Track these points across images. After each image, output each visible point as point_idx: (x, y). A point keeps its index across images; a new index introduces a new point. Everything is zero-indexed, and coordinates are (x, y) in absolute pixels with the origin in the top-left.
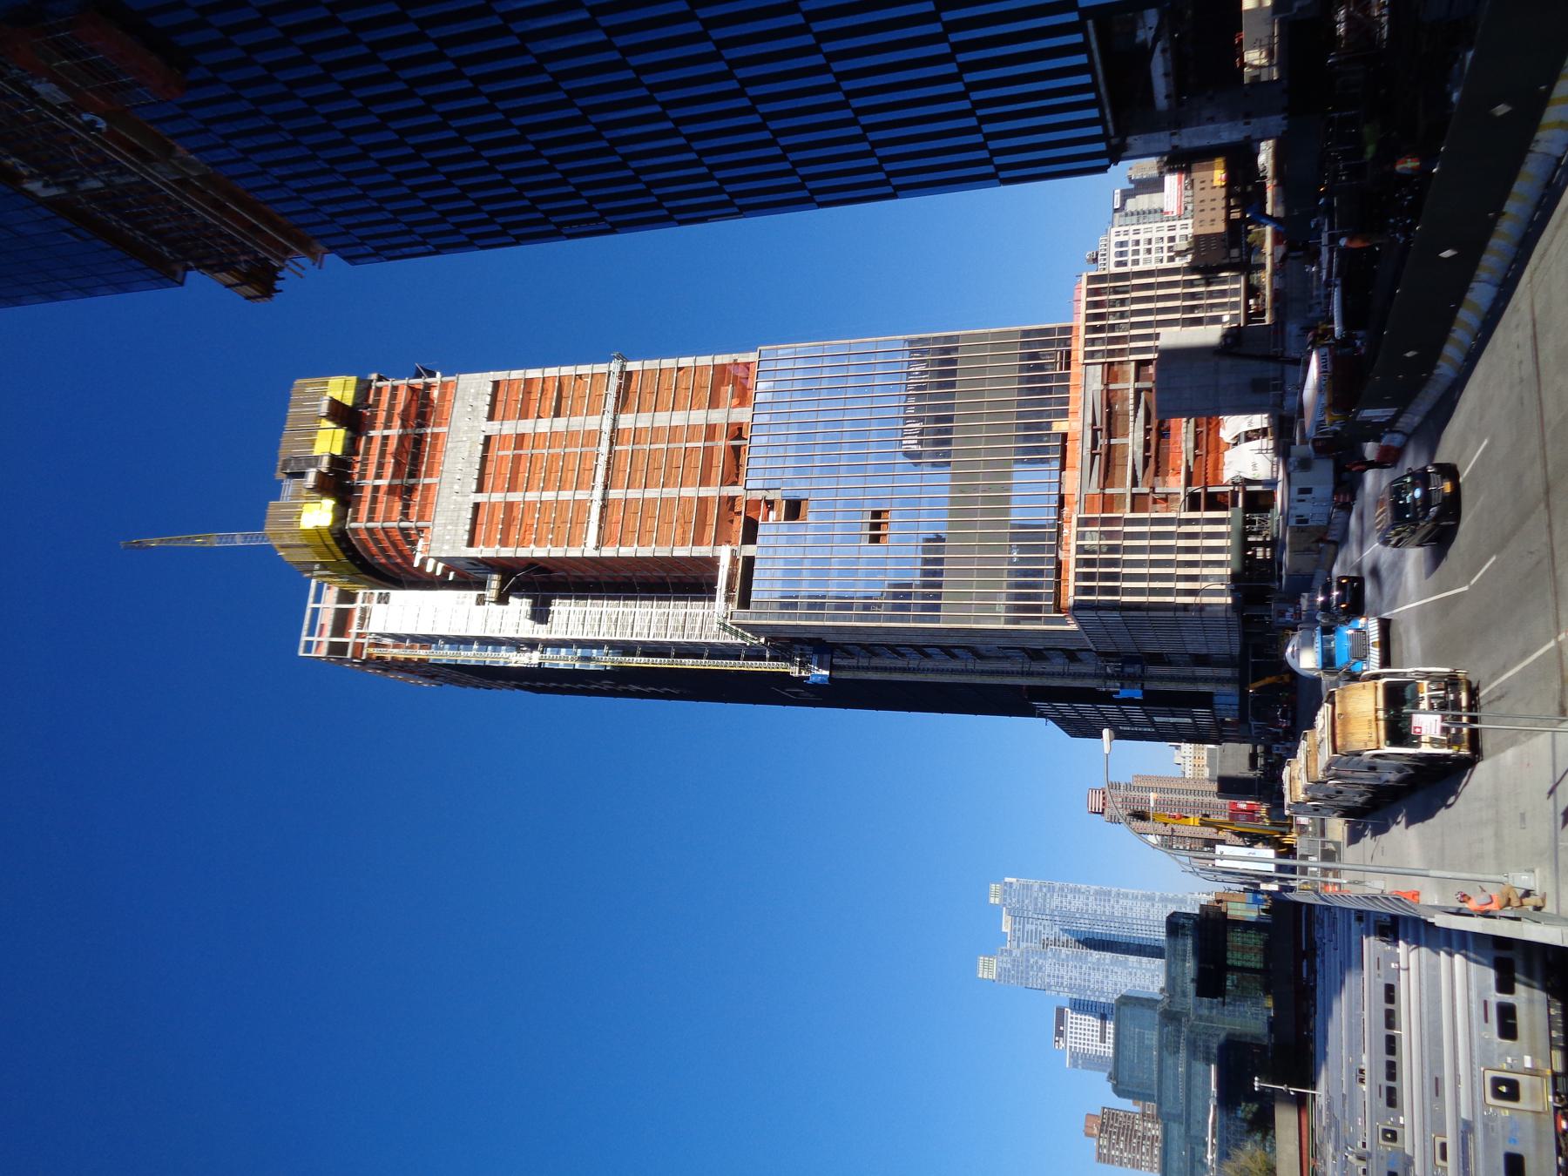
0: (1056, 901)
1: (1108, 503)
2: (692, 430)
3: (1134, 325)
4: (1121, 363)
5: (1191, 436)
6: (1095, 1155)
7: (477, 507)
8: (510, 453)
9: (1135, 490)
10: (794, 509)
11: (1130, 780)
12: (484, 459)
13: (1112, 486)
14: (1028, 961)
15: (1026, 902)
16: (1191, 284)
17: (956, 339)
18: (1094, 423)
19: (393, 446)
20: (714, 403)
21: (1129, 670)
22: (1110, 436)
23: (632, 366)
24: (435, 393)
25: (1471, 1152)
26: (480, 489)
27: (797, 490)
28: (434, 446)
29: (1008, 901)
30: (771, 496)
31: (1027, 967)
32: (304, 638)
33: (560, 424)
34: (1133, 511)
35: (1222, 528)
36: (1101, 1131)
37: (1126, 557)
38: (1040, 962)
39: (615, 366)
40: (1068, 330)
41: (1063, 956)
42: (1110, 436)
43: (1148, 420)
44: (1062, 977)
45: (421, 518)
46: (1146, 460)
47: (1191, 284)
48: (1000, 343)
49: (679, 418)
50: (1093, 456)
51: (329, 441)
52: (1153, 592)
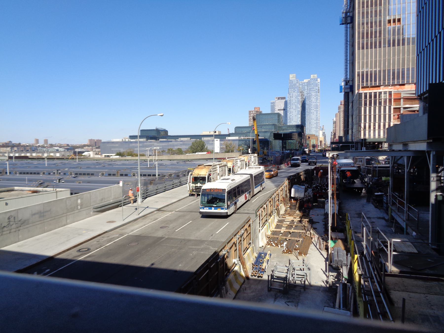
0: (313, 94)
6: (250, 110)
9: (402, 109)
13: (403, 101)
14: (296, 88)
15: (312, 86)
31: (294, 88)
36: (256, 111)
38: (296, 91)
41: (298, 98)
44: (293, 98)
52: (365, 116)
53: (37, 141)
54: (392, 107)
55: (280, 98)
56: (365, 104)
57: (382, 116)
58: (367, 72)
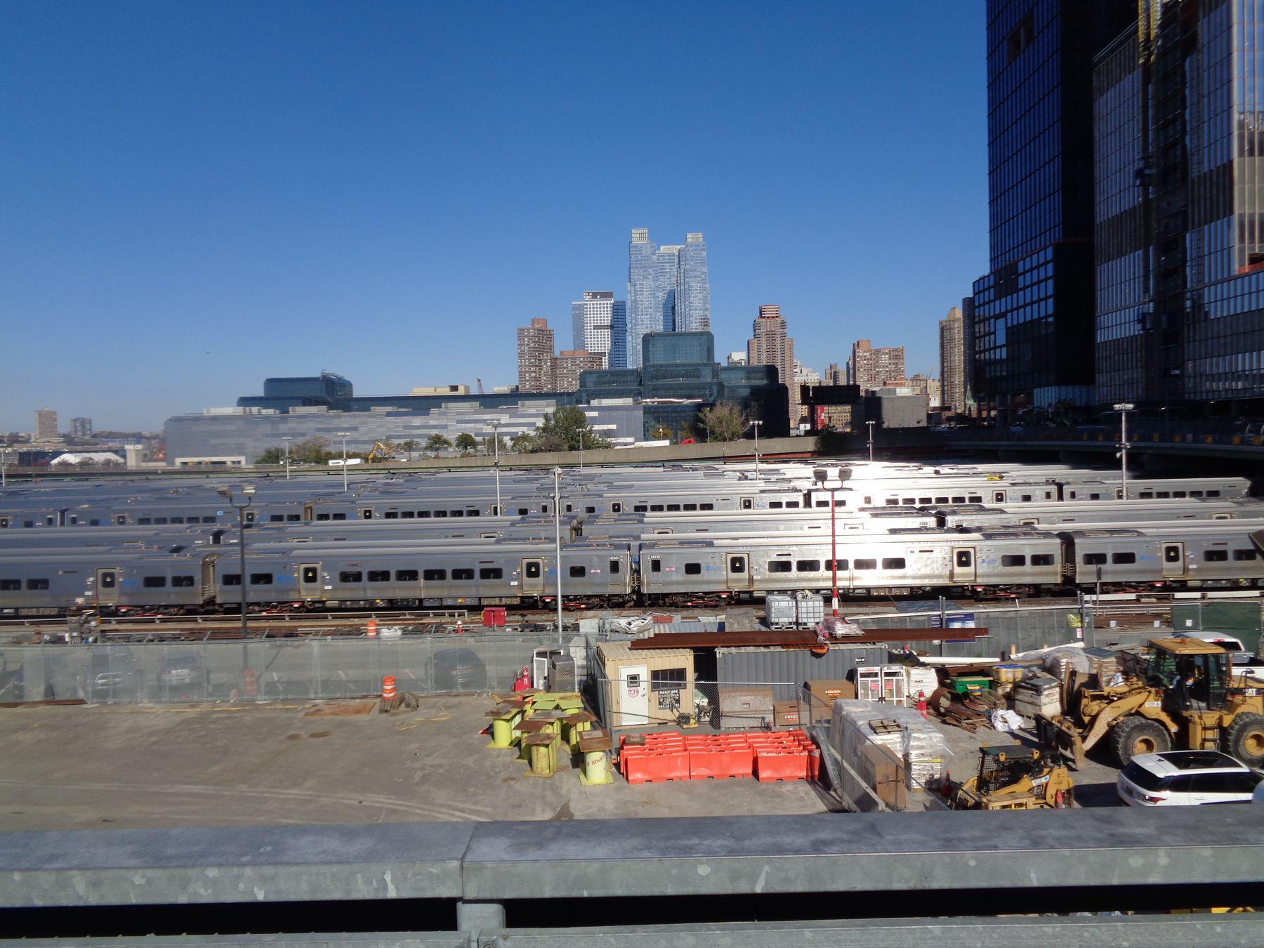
0: (696, 285)
6: (522, 327)
11: (788, 336)
14: (650, 267)
15: (692, 263)
21: (1164, 318)
25: (1126, 535)
31: (646, 267)
36: (538, 330)
38: (650, 277)
41: (657, 294)
44: (642, 294)
53: (835, 376)
55: (599, 293)
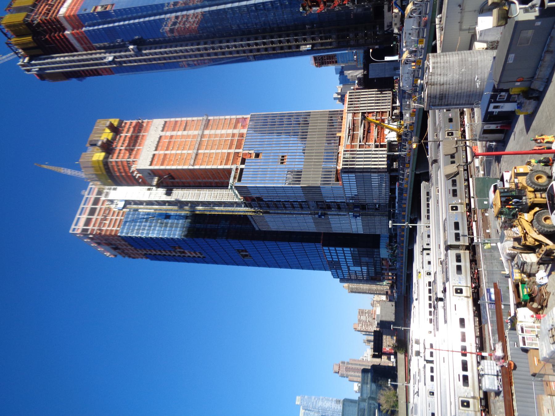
0: (320, 404)
1: (352, 146)
2: (228, 135)
3: (361, 104)
4: (357, 113)
5: (376, 132)
7: (154, 155)
8: (167, 140)
9: (360, 144)
10: (257, 155)
11: (348, 361)
12: (159, 142)
15: (309, 404)
16: (377, 94)
17: (310, 112)
18: (349, 127)
19: (134, 124)
20: (235, 127)
21: (355, 209)
22: (353, 131)
23: (210, 118)
24: (145, 125)
25: (446, 225)
26: (156, 150)
27: (259, 149)
28: (142, 139)
29: (303, 403)
30: (250, 152)
32: (73, 227)
33: (185, 133)
34: (359, 148)
35: (384, 156)
37: (357, 160)
39: (205, 118)
40: (343, 111)
42: (353, 131)
43: (364, 127)
45: (135, 158)
46: (364, 138)
47: (377, 94)
48: (322, 114)
49: (224, 132)
50: (349, 136)
51: (107, 135)
53: (369, 341)
54: (358, 149)
56: (354, 165)
57: (365, 156)
58: (323, 171)
